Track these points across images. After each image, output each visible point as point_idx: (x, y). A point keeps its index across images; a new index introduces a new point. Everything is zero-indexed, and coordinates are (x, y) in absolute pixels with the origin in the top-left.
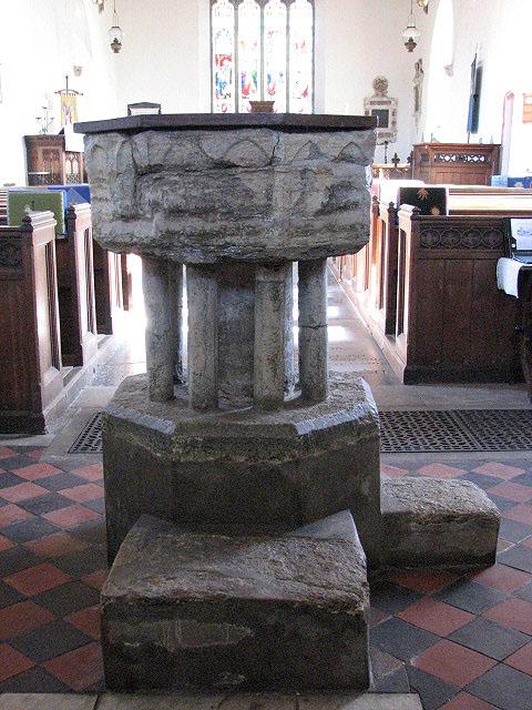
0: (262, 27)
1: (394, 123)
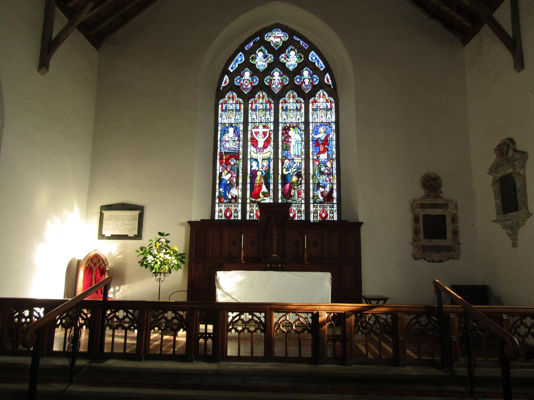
0: (276, 123)
1: (455, 233)
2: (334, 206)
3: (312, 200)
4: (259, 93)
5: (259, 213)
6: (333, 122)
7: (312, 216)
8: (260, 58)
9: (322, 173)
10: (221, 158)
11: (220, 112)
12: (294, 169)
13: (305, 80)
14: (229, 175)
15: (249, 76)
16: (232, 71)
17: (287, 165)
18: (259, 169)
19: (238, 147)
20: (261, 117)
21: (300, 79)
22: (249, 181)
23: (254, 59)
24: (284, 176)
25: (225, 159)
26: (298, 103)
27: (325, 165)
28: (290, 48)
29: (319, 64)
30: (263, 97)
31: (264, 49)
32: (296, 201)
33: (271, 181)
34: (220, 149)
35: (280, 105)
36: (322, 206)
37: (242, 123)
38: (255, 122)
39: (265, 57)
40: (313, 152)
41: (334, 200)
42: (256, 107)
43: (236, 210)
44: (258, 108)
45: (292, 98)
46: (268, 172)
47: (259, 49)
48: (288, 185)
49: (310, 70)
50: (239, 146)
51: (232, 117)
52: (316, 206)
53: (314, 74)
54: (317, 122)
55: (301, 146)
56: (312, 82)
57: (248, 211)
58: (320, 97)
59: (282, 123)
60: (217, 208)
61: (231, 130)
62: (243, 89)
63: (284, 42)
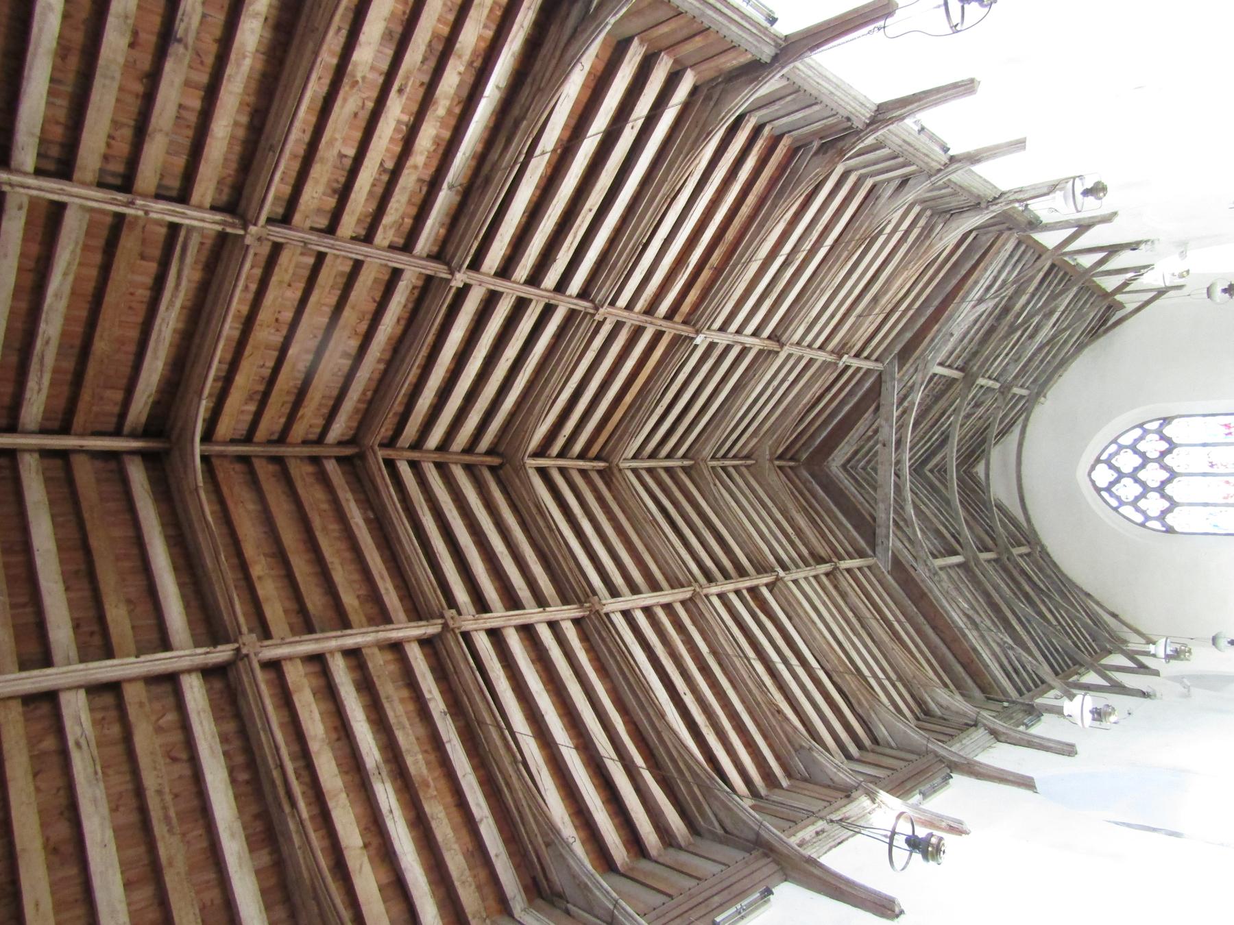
0: (1204, 474)
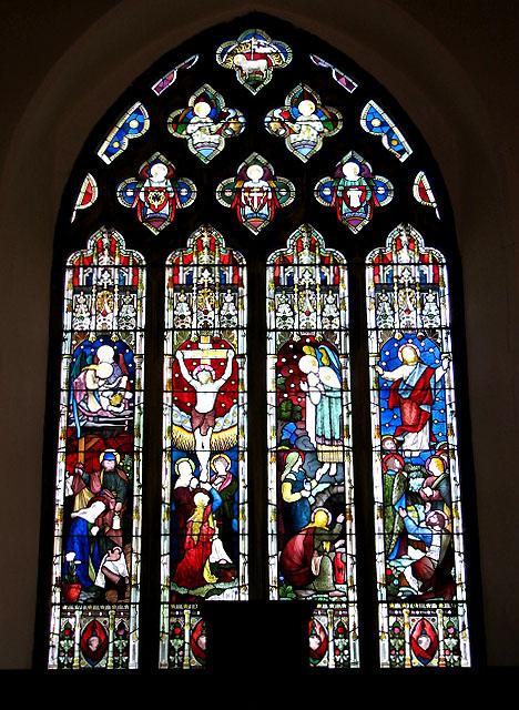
0: (257, 331)
2: (460, 611)
3: (384, 590)
4: (198, 234)
5: (203, 640)
6: (446, 328)
7: (384, 644)
8: (200, 122)
9: (413, 498)
10: (71, 450)
11: (68, 294)
12: (318, 483)
13: (349, 193)
14: (99, 507)
15: (166, 177)
16: (108, 161)
17: (295, 469)
18: (202, 486)
19: (129, 412)
20: (206, 312)
21: (334, 190)
22: (165, 525)
23: (182, 122)
24: (282, 506)
25: (85, 452)
26: (328, 266)
27: (424, 471)
28: (298, 90)
29: (395, 143)
30: (212, 247)
31: (214, 91)
32: (327, 593)
33: (243, 525)
34: (68, 418)
35: (270, 274)
36: (418, 612)
37: (141, 330)
38: (187, 326)
39: (217, 116)
40: (380, 427)
41: (459, 589)
42: (189, 278)
43: (122, 626)
44: (195, 281)
45: (306, 251)
46: (230, 494)
47: (198, 94)
48: (300, 539)
49: (366, 159)
50: (132, 409)
51: (108, 311)
52: (396, 612)
53: (374, 174)
54: (391, 329)
55: (340, 405)
56: (371, 198)
57: (163, 632)
58: (398, 245)
59: (276, 330)
60: (55, 624)
61: (106, 353)
62: (146, 221)
63: (277, 72)
